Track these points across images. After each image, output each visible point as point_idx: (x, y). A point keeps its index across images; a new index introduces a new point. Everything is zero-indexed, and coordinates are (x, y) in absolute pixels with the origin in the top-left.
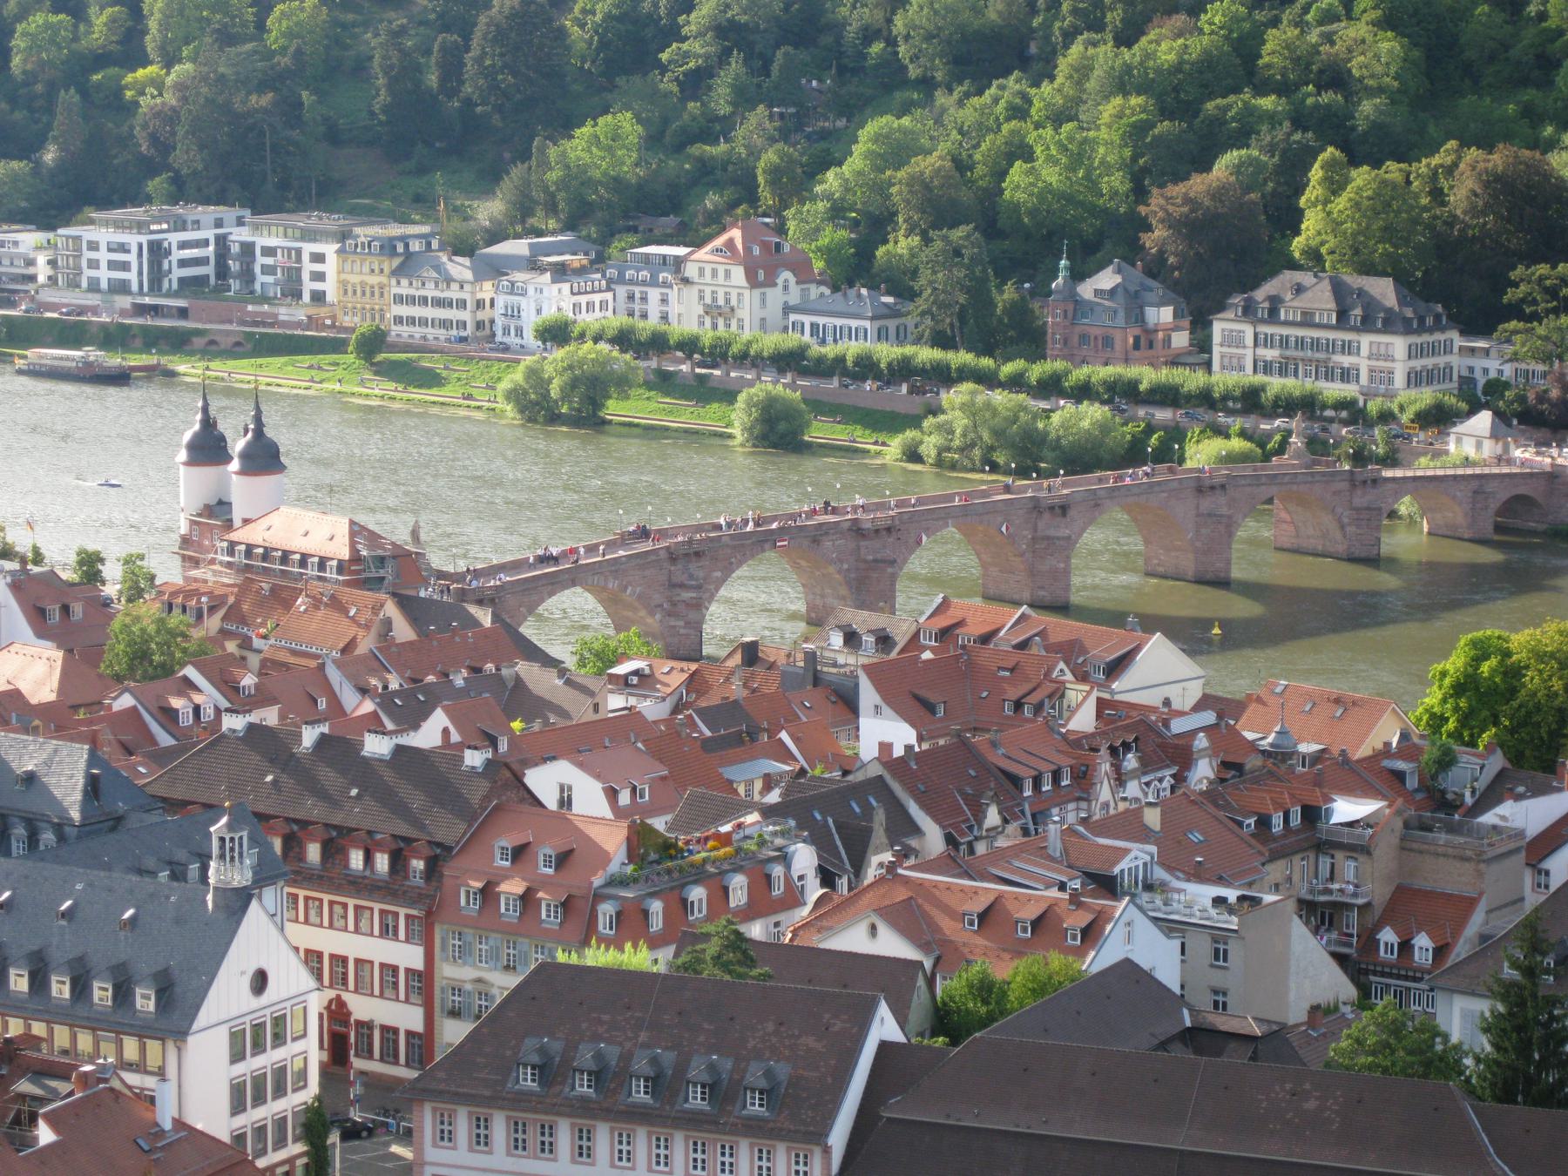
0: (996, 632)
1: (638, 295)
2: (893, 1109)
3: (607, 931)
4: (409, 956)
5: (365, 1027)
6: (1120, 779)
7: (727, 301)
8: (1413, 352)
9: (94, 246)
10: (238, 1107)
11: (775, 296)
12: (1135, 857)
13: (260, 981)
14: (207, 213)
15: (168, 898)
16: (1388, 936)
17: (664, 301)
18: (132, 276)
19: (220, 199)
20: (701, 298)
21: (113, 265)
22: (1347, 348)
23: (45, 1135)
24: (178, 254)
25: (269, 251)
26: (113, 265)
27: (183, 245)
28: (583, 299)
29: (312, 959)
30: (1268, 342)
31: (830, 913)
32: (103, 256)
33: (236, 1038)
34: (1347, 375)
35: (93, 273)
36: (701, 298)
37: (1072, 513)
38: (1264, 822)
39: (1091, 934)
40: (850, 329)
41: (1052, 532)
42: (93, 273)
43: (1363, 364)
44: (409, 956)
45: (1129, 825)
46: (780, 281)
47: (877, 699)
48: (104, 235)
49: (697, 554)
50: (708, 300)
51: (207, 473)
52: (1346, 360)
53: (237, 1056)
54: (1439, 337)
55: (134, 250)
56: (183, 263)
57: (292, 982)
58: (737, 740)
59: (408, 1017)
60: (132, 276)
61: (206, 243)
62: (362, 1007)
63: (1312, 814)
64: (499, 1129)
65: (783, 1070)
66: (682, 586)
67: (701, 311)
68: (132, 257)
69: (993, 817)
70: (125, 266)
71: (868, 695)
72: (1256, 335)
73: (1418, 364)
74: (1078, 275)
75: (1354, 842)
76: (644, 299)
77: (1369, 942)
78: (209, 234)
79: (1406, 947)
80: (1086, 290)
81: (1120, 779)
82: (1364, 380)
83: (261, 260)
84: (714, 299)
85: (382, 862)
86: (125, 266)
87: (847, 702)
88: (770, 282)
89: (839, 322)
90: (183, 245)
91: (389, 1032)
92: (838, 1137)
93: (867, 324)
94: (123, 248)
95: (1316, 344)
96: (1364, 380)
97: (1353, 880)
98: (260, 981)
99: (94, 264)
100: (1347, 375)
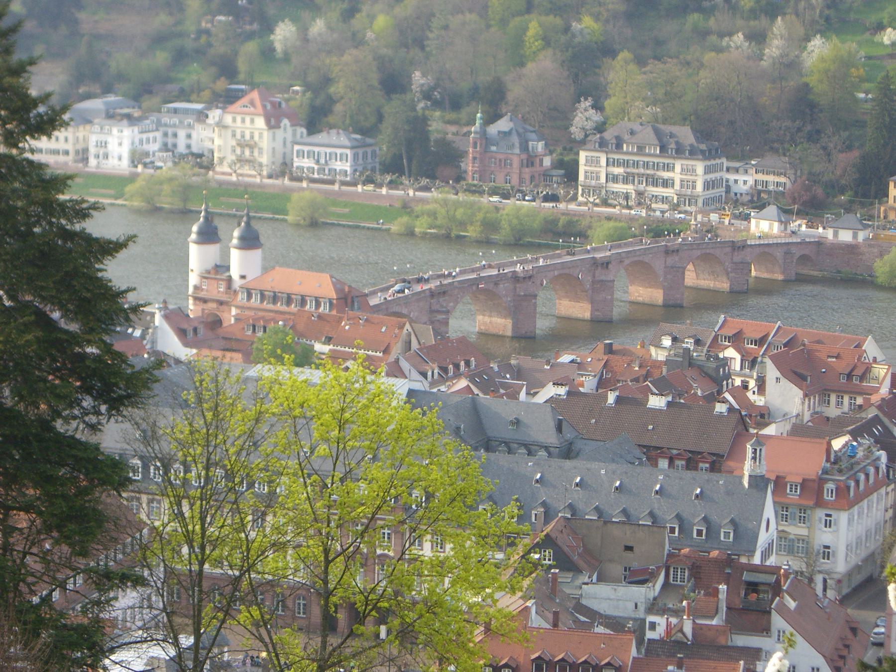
0: (767, 336)
1: (170, 133)
3: (830, 498)
7: (252, 137)
8: (708, 170)
11: (280, 133)
15: (718, 482)
17: (189, 136)
20: (234, 135)
22: (669, 168)
28: (144, 136)
30: (618, 164)
34: (666, 183)
36: (234, 135)
37: (610, 266)
40: (314, 152)
41: (603, 278)
43: (676, 175)
46: (282, 125)
47: (778, 374)
49: (444, 293)
50: (238, 136)
51: (213, 250)
52: (666, 175)
54: (718, 161)
66: (438, 312)
67: (234, 143)
72: (607, 159)
73: (712, 176)
76: (175, 135)
80: (493, 129)
82: (677, 186)
84: (243, 136)
88: (278, 126)
89: (328, 150)
93: (348, 152)
95: (646, 165)
96: (677, 186)
100: (666, 183)
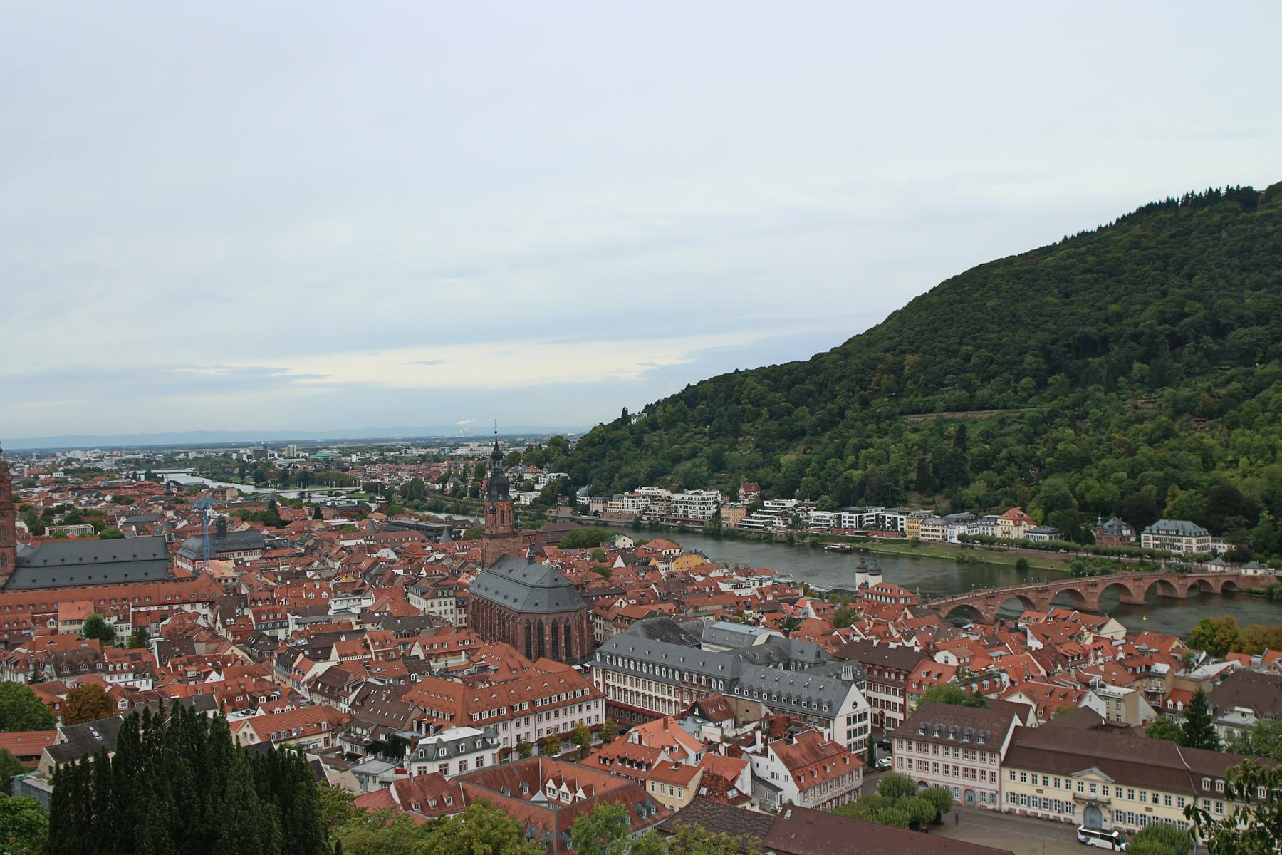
2: (1018, 743)
4: (900, 700)
5: (889, 719)
6: (1096, 658)
10: (849, 737)
11: (1022, 528)
12: (1096, 679)
13: (855, 704)
14: (874, 509)
16: (1170, 702)
19: (878, 505)
23: (795, 741)
29: (872, 702)
31: (1011, 691)
33: (849, 719)
38: (1134, 669)
39: (1080, 698)
44: (900, 700)
45: (1095, 670)
48: (847, 514)
53: (849, 724)
57: (863, 706)
58: (994, 646)
59: (900, 716)
62: (888, 713)
63: (1148, 668)
64: (914, 745)
65: (988, 732)
69: (1059, 667)
71: (1029, 634)
74: (1104, 521)
75: (1161, 676)
77: (1165, 704)
79: (1175, 705)
80: (1106, 525)
81: (1096, 658)
85: (893, 676)
87: (1025, 634)
91: (895, 720)
92: (1003, 750)
97: (1164, 687)
98: (855, 704)
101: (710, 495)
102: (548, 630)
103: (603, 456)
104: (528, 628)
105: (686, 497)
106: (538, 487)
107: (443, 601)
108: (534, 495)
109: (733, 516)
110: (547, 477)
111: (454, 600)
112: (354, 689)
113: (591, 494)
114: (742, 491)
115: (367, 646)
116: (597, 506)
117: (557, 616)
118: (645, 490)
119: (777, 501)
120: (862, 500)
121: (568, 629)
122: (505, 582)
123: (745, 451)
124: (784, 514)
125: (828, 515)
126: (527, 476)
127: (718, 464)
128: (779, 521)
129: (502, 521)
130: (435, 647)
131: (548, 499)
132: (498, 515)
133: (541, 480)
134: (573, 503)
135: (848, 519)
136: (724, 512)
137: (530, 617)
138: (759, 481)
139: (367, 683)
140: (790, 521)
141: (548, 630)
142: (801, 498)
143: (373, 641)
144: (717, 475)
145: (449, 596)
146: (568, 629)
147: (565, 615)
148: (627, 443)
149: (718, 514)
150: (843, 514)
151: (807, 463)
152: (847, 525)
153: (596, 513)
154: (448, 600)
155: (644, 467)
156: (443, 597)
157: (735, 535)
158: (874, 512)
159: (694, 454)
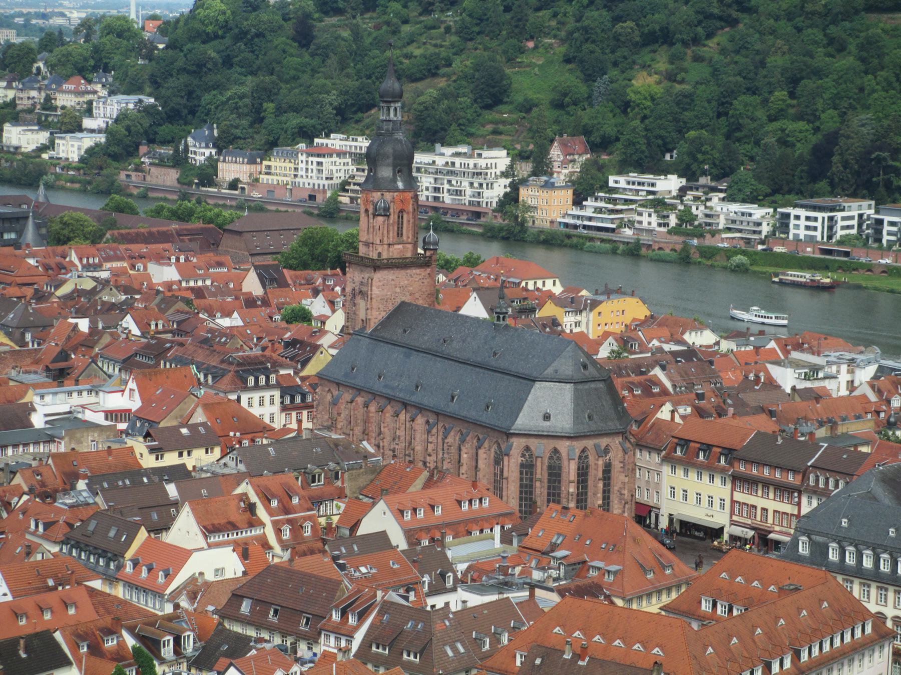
9: (797, 217)
14: (855, 204)
18: (818, 234)
21: (808, 228)
24: (840, 223)
25: (892, 224)
26: (808, 228)
27: (843, 219)
32: (803, 223)
35: (796, 232)
42: (796, 232)
48: (803, 213)
55: (820, 220)
56: (843, 228)
60: (818, 234)
61: (852, 218)
68: (818, 224)
70: (815, 229)
78: (855, 213)
83: (886, 228)
86: (815, 229)
90: (843, 219)
94: (816, 219)
99: (797, 227)
101: (498, 159)
102: (571, 470)
103: (228, 62)
104: (527, 468)
105: (440, 161)
106: (87, 123)
107: (256, 396)
108: (88, 142)
109: (550, 206)
110: (109, 108)
111: (277, 394)
112: (362, 617)
113: (223, 144)
114: (555, 153)
115: (251, 508)
116: (231, 169)
117: (589, 443)
118: (336, 141)
119: (633, 176)
120: (823, 185)
121: (607, 470)
122: (439, 364)
123: (537, 72)
124: (659, 205)
125: (758, 212)
126: (65, 100)
127: (492, 93)
128: (649, 220)
129: (400, 234)
130: (421, 515)
131: (122, 145)
132: (393, 218)
133: (99, 109)
134: (180, 161)
135: (805, 224)
136: (525, 194)
137: (533, 443)
138: (587, 132)
139: (387, 606)
140: (673, 221)
141: (571, 470)
142: (689, 173)
143: (266, 499)
144: (489, 115)
145: (268, 386)
146: (607, 470)
147: (604, 442)
148: (280, 40)
149: (511, 198)
150: (793, 212)
151: (686, 101)
152: (802, 233)
153: (234, 185)
154: (267, 394)
155: (331, 90)
156: (257, 387)
157: (551, 240)
158: (855, 212)
159: (431, 70)
